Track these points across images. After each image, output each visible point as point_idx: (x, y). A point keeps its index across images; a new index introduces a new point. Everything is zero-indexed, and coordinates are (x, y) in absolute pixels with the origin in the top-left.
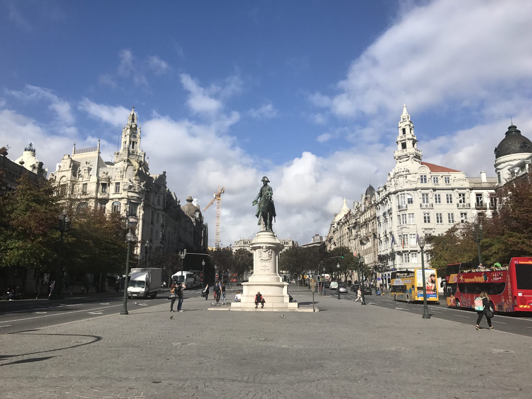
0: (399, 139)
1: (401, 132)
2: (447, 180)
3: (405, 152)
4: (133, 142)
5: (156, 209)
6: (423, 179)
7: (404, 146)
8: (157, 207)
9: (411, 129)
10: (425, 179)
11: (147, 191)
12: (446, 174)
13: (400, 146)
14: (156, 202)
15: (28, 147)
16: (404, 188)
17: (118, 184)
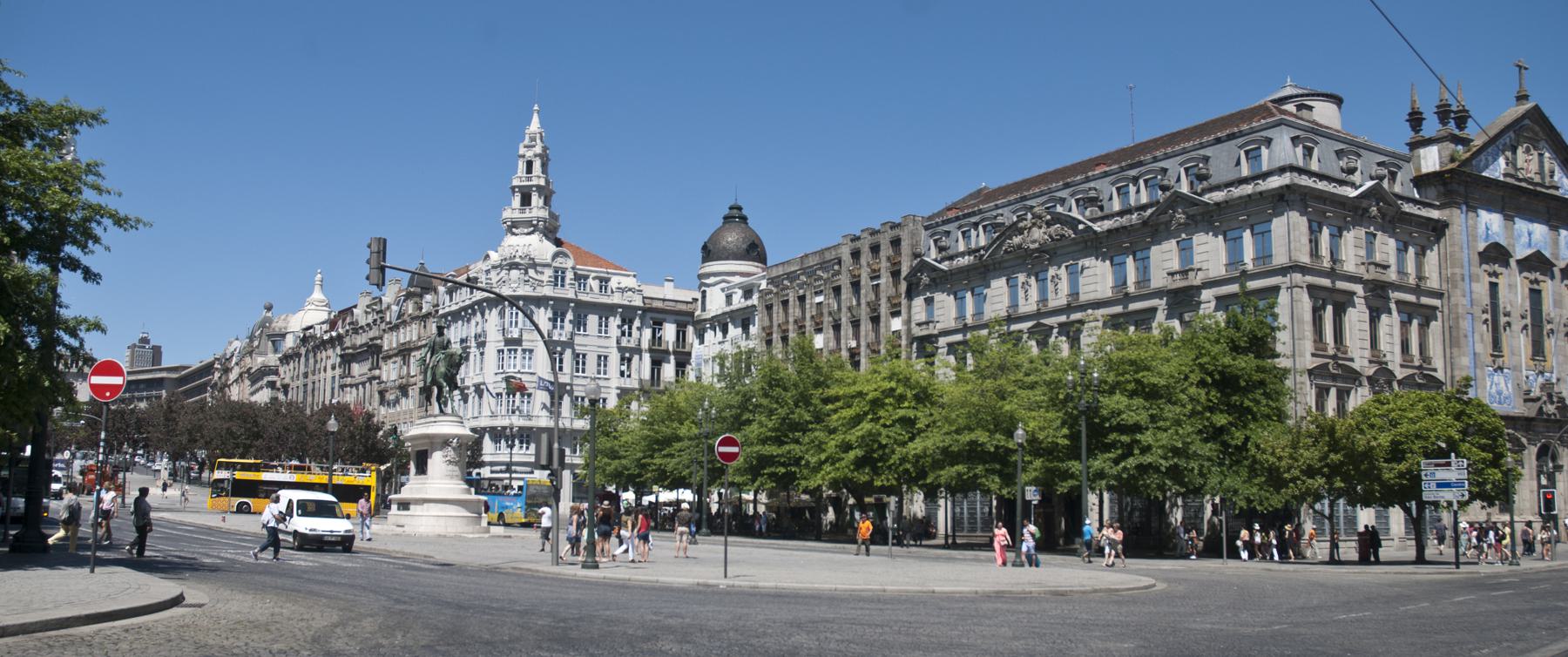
0: (516, 182)
1: (522, 166)
2: (604, 281)
3: (527, 215)
6: (558, 278)
7: (526, 201)
10: (563, 279)
12: (602, 271)
13: (516, 201)
16: (520, 292)
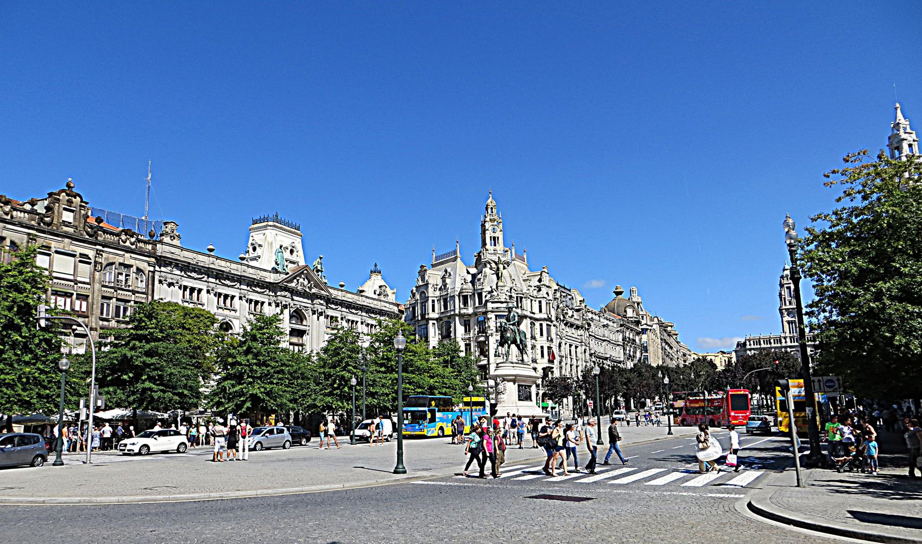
4: (494, 238)
5: (537, 320)
8: (538, 316)
9: (910, 146)
11: (521, 298)
14: (536, 309)
15: (373, 268)
17: (480, 295)
